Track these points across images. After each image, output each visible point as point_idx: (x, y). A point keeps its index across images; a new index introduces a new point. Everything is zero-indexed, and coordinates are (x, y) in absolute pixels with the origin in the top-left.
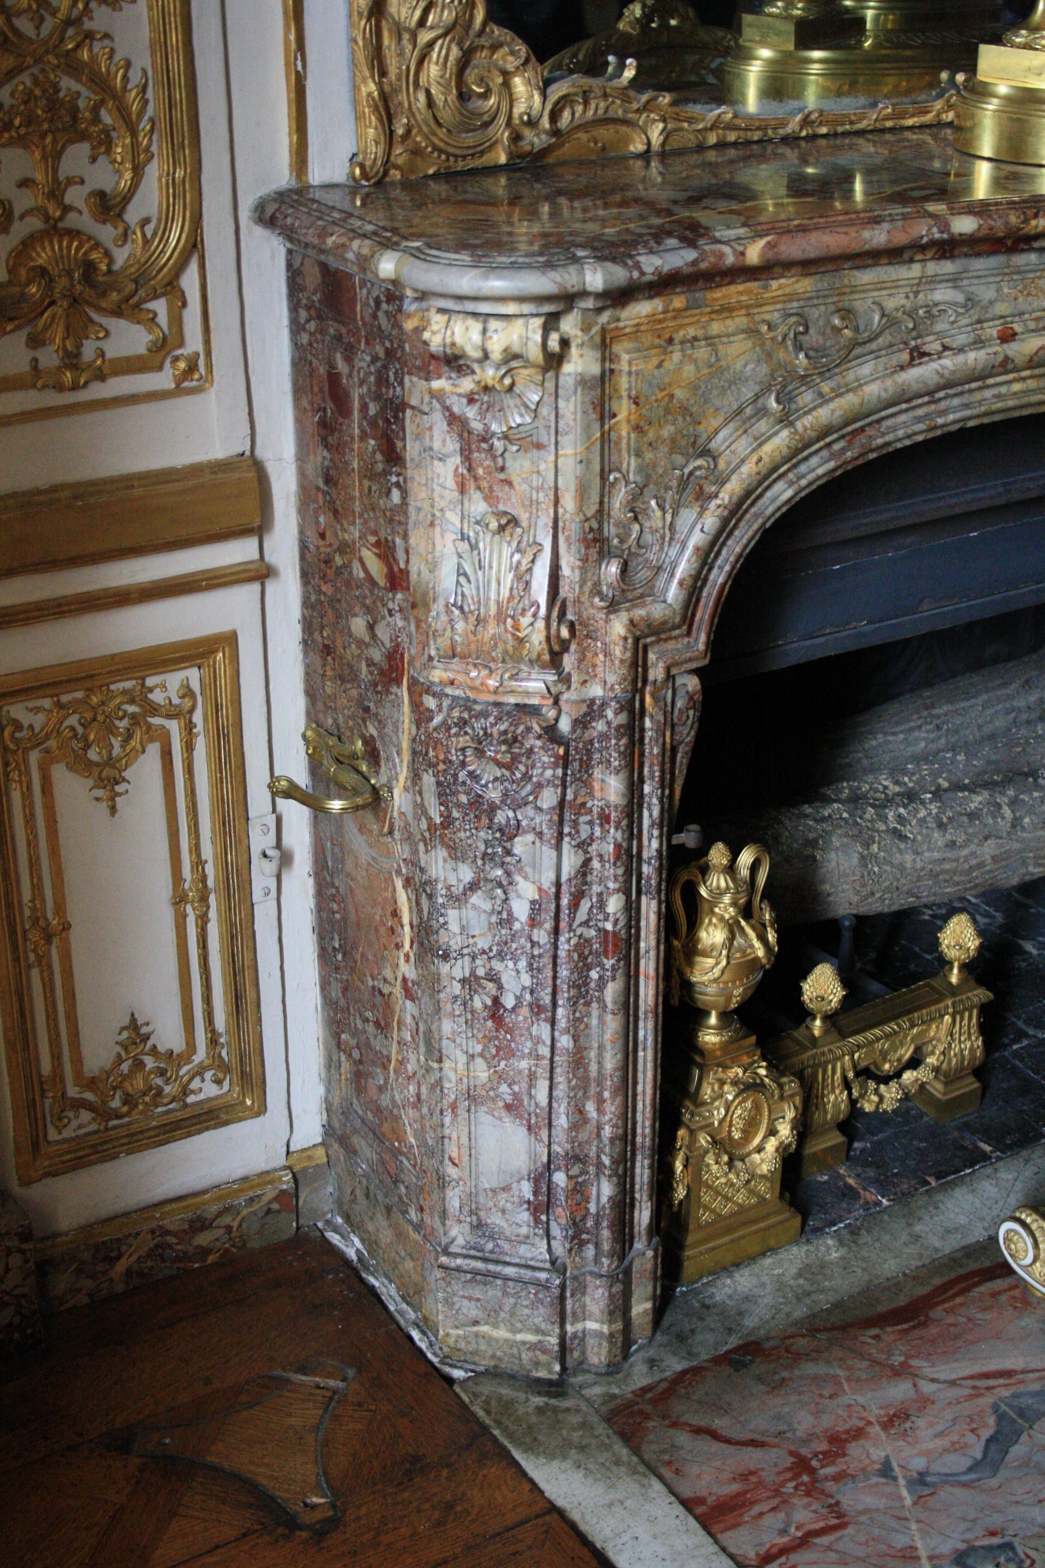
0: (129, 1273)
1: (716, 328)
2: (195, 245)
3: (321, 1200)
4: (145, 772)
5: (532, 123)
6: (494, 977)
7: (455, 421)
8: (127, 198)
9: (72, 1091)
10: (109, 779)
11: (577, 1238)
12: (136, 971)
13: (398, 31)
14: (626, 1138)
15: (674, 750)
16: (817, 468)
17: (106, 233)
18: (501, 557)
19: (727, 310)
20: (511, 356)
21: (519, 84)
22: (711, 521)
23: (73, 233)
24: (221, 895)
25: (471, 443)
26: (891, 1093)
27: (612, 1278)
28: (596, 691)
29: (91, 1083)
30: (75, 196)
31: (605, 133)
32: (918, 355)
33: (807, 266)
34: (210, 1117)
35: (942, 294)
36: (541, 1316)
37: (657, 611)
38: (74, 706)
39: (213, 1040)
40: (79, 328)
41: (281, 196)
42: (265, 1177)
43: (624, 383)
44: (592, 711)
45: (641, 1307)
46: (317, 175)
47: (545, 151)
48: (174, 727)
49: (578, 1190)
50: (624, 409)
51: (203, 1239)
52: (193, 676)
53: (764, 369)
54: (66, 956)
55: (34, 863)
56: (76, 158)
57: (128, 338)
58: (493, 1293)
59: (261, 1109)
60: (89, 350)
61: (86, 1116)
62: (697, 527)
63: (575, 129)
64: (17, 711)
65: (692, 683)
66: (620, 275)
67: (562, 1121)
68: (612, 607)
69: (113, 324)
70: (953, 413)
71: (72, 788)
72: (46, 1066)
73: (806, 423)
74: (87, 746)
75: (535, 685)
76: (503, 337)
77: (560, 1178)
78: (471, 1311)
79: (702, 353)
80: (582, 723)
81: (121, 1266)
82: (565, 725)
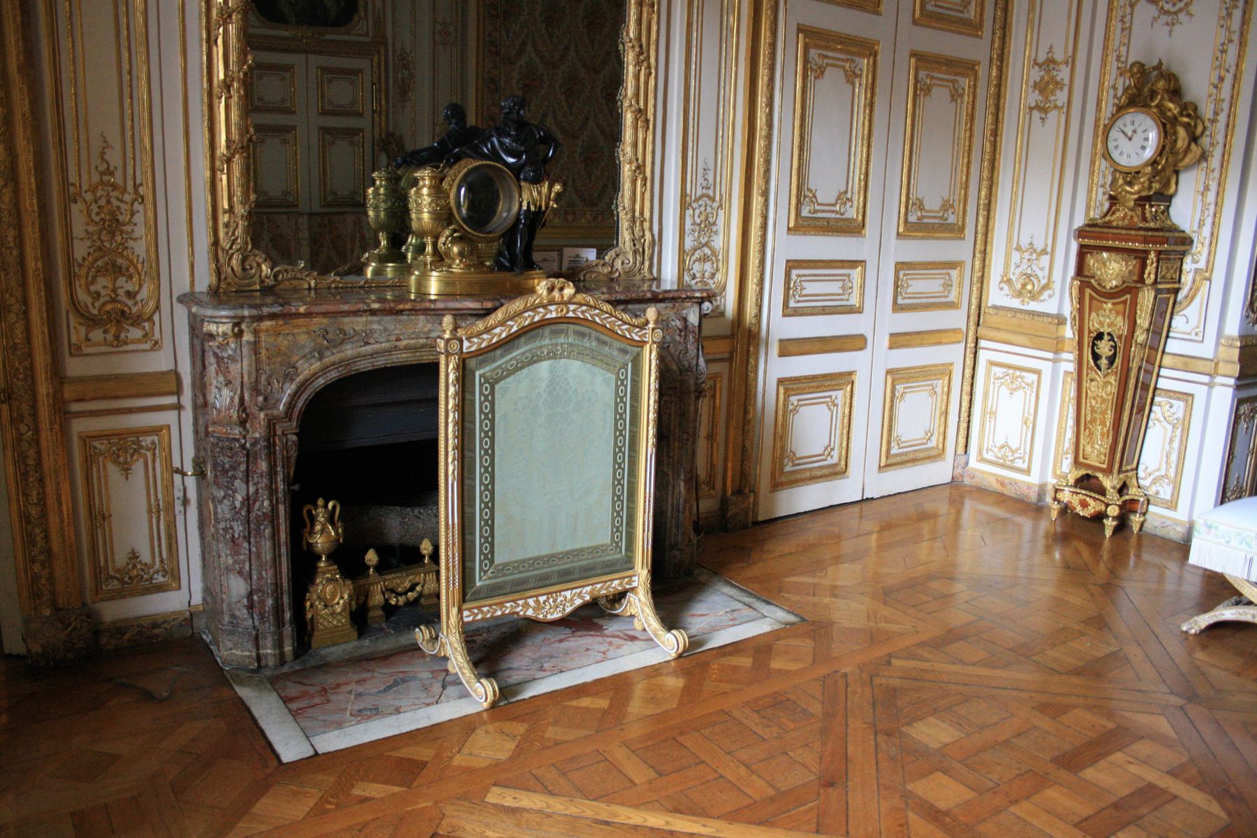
0: (129, 640)
1: (295, 331)
2: (158, 307)
3: (200, 623)
4: (138, 467)
5: (266, 277)
6: (232, 528)
7: (215, 354)
8: (137, 293)
9: (111, 573)
10: (126, 469)
11: (262, 617)
12: (134, 535)
13: (223, 249)
14: (277, 585)
15: (289, 458)
16: (334, 375)
17: (130, 303)
18: (226, 393)
19: (298, 326)
20: (225, 334)
21: (264, 267)
22: (293, 387)
23: (119, 302)
26: (402, 600)
27: (274, 634)
28: (257, 435)
29: (118, 571)
30: (121, 292)
31: (295, 282)
32: (367, 343)
34: (161, 588)
35: (375, 326)
36: (250, 645)
37: (275, 412)
38: (115, 444)
39: (162, 561)
40: (120, 329)
41: (185, 295)
42: (180, 613)
43: (263, 345)
44: (256, 442)
45: (288, 648)
47: (273, 286)
48: (149, 454)
49: (262, 602)
50: (264, 352)
51: (156, 631)
52: (156, 438)
53: (312, 344)
54: (110, 527)
55: (100, 493)
56: (121, 281)
57: (135, 333)
58: (235, 638)
59: (179, 588)
60: (123, 336)
61: (116, 582)
62: (290, 389)
63: (283, 280)
64: (96, 444)
65: (295, 438)
66: (254, 312)
67: (255, 577)
68: (261, 409)
69: (131, 329)
70: (381, 362)
71: (113, 471)
72: (102, 564)
73: (327, 361)
74: (119, 456)
75: (237, 431)
76: (222, 329)
77: (255, 597)
78: (230, 645)
79: (290, 338)
80: (253, 445)
81: (127, 637)
82: (248, 445)
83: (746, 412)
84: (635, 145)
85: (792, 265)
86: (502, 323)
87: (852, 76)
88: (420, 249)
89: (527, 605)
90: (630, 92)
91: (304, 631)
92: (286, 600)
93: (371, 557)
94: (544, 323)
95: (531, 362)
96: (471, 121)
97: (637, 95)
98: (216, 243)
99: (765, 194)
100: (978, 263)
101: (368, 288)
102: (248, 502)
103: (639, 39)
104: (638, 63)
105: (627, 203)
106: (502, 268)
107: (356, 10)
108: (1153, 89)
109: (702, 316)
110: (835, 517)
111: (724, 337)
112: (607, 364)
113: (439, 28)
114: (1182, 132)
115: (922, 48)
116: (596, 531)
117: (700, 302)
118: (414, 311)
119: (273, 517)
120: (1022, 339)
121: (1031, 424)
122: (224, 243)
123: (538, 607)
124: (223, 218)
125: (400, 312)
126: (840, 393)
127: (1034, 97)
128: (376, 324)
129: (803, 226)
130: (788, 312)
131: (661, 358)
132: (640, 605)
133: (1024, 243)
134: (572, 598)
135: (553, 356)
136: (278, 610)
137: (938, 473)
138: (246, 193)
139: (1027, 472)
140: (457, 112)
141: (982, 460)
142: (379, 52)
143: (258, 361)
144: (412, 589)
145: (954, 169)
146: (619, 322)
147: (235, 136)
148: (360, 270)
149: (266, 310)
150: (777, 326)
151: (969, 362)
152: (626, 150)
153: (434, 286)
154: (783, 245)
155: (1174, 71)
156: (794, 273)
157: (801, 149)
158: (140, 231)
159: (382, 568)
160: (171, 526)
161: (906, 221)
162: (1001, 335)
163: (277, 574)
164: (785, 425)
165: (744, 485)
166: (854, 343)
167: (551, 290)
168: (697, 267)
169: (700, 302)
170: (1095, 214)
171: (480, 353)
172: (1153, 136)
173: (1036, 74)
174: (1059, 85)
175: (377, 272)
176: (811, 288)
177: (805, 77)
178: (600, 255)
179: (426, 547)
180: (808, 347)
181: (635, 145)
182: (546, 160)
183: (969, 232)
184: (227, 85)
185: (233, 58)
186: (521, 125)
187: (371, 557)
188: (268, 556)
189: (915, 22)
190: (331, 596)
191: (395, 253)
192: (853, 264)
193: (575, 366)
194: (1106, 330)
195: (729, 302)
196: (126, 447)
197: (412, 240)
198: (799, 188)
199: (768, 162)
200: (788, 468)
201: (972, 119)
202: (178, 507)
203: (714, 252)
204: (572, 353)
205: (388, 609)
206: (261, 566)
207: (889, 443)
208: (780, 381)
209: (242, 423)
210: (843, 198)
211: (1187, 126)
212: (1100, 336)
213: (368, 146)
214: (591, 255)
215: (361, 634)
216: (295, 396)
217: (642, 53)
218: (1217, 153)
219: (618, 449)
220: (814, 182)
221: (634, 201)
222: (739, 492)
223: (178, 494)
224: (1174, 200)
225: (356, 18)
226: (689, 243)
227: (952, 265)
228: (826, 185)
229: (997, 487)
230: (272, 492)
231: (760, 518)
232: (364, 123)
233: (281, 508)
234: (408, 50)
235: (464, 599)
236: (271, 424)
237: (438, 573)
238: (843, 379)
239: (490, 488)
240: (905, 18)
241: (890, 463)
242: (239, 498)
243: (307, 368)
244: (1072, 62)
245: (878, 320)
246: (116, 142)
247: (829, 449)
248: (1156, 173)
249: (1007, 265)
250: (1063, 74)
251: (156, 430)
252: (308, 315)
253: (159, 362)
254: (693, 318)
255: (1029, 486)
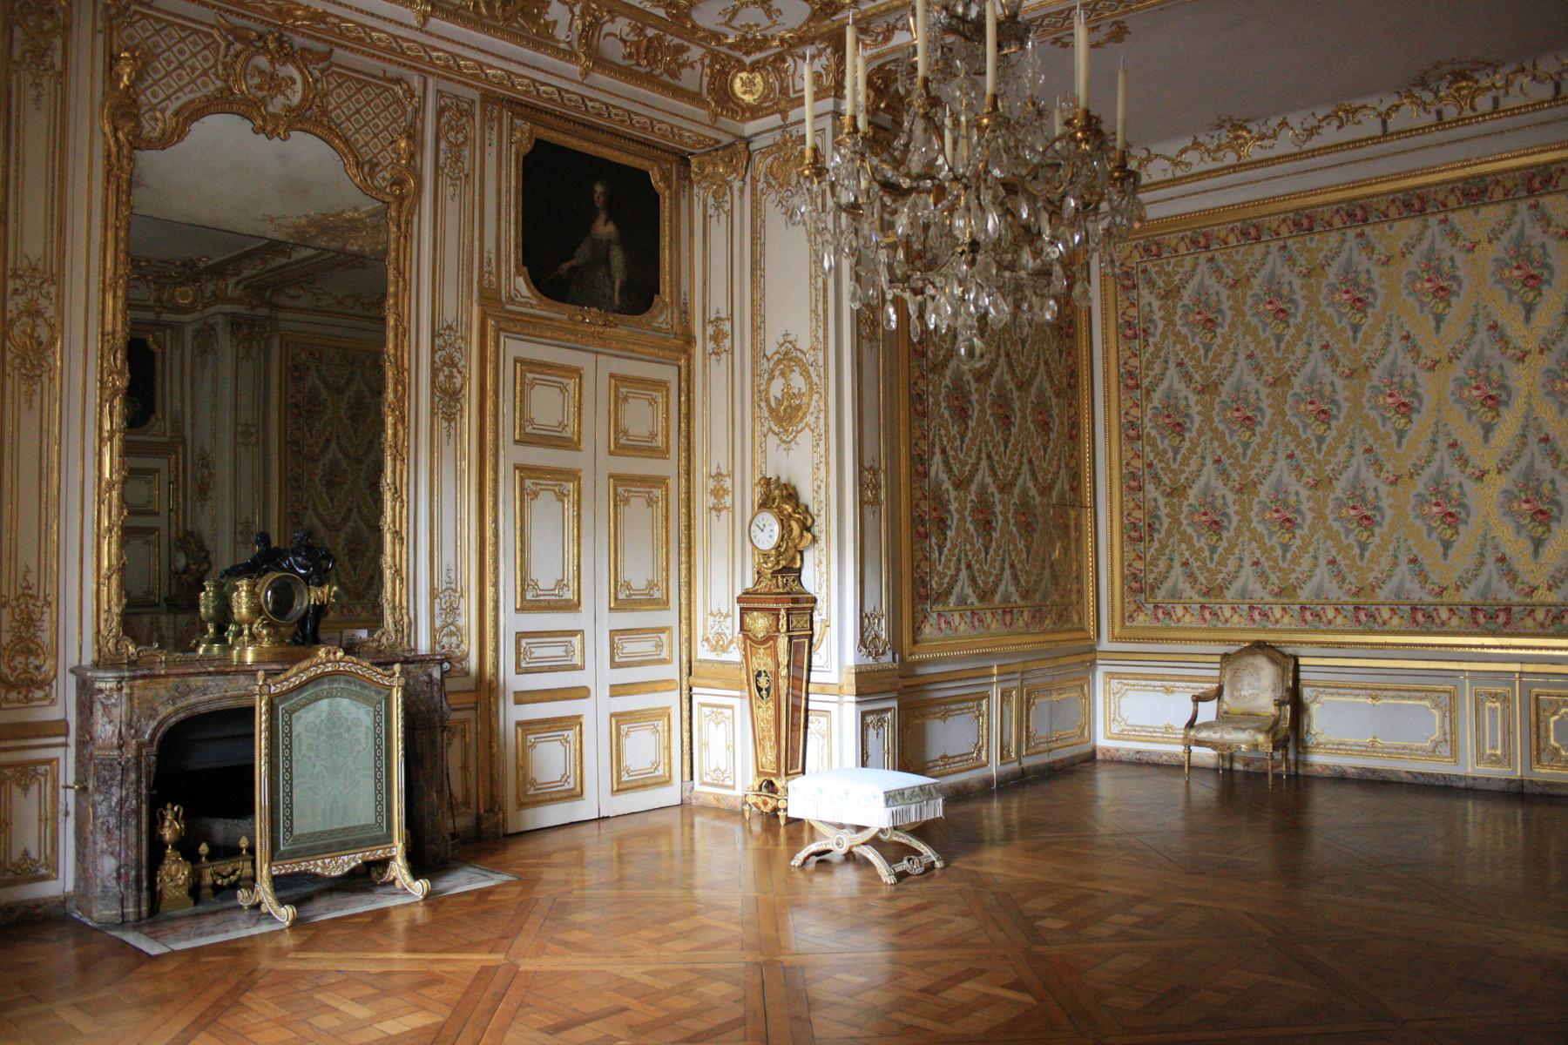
2: (56, 676)
3: (71, 905)
4: (34, 789)
10: (25, 789)
11: (127, 887)
14: (138, 861)
16: (182, 715)
18: (109, 728)
24: (50, 820)
25: (105, 706)
26: (226, 881)
33: (177, 675)
34: (44, 878)
36: (117, 906)
40: (29, 691)
44: (128, 760)
45: (144, 908)
46: (84, 663)
49: (127, 873)
56: (31, 659)
57: (39, 694)
62: (153, 724)
70: (214, 707)
71: (16, 791)
75: (116, 753)
83: (491, 748)
84: (394, 556)
85: (520, 636)
86: (296, 675)
87: (561, 496)
88: (240, 633)
89: (316, 865)
90: (389, 520)
91: (155, 898)
92: (144, 872)
93: (204, 848)
94: (324, 675)
95: (317, 700)
96: (274, 544)
97: (394, 522)
98: (98, 632)
99: (496, 585)
100: (684, 627)
101: (201, 660)
102: (121, 802)
103: (394, 483)
104: (394, 500)
105: (389, 595)
106: (296, 643)
107: (153, 412)
108: (781, 497)
109: (443, 673)
110: (577, 829)
111: (469, 691)
112: (367, 701)
113: (240, 429)
114: (794, 525)
115: (619, 471)
116: (362, 812)
117: (441, 662)
118: (237, 672)
119: (138, 812)
120: (718, 683)
121: (731, 748)
122: (104, 632)
123: (325, 867)
124: (103, 616)
125: (228, 673)
126: (571, 733)
127: (712, 501)
128: (210, 682)
129: (526, 607)
130: (520, 670)
131: (404, 696)
132: (399, 869)
133: (715, 611)
134: (347, 862)
135: (330, 695)
136: (138, 879)
137: (669, 796)
138: (120, 599)
139: (733, 788)
140: (264, 538)
141: (703, 783)
142: (176, 452)
143: (132, 707)
144: (233, 873)
145: (655, 557)
146: (377, 675)
147: (114, 562)
148: (194, 650)
149: (139, 673)
150: (514, 682)
151: (686, 706)
152: (387, 560)
153: (250, 657)
154: (511, 621)
155: (793, 482)
156: (524, 642)
157: (522, 551)
158: (46, 625)
159: (211, 857)
160: (55, 831)
161: (616, 599)
162: (705, 682)
163: (139, 853)
164: (525, 756)
165: (494, 804)
166: (581, 693)
167: (328, 653)
168: (445, 641)
169: (441, 662)
170: (749, 585)
171: (282, 694)
172: (776, 528)
173: (711, 484)
174: (726, 492)
175: (206, 650)
176: (538, 652)
177: (522, 501)
178: (371, 633)
179: (244, 843)
180: (538, 696)
181: (394, 556)
182: (327, 570)
183: (674, 603)
184: (110, 530)
185: (114, 512)
186: (309, 548)
187: (204, 848)
188: (133, 840)
189: (611, 453)
190: (176, 873)
191: (220, 637)
192: (573, 633)
193: (345, 703)
194: (762, 669)
195: (473, 663)
196: (26, 773)
197: (232, 628)
198: (523, 580)
199: (496, 561)
200: (531, 792)
201: (667, 518)
202: (61, 817)
203: (458, 629)
204: (343, 694)
205: (217, 889)
206: (128, 847)
207: (619, 772)
208: (519, 724)
209: (120, 747)
210: (561, 584)
211: (798, 520)
212: (759, 674)
213: (164, 547)
214: (363, 634)
215: (196, 904)
216: (156, 730)
217: (397, 493)
218: (823, 536)
219: (377, 758)
220: (535, 573)
221: (394, 594)
222: (490, 810)
223: (61, 807)
224: (804, 572)
225: (153, 419)
226: (438, 623)
227: (662, 630)
228: (545, 575)
229: (715, 803)
230: (138, 795)
231: (510, 831)
232: (161, 522)
233: (144, 807)
234: (208, 449)
235: (272, 859)
236: (140, 747)
237: (254, 862)
238: (574, 721)
239: (290, 770)
240: (602, 451)
241: (620, 789)
242: (115, 799)
243: (164, 711)
244: (732, 474)
245: (598, 674)
246: (34, 567)
247: (565, 777)
248: (779, 554)
249: (705, 627)
250: (728, 484)
251: (49, 762)
252: (166, 676)
253: (54, 713)
254: (436, 674)
255: (735, 798)
